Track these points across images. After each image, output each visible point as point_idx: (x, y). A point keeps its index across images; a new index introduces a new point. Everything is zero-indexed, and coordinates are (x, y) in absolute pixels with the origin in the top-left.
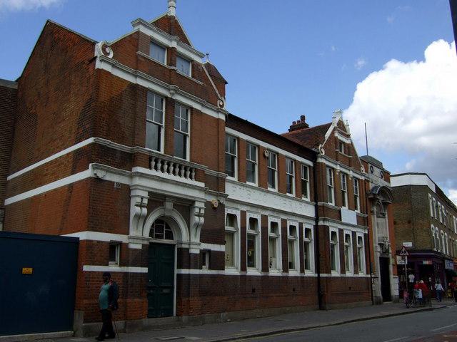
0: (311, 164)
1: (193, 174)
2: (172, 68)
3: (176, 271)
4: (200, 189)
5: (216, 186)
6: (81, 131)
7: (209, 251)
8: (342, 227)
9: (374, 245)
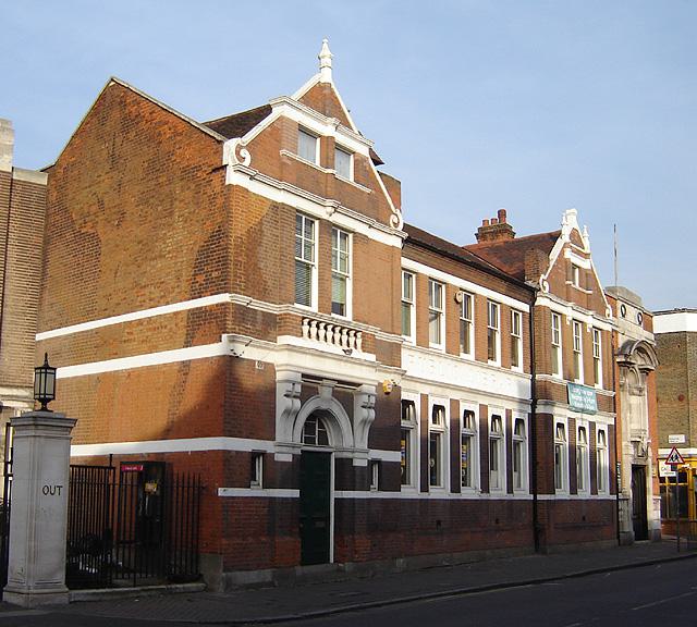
0: (526, 308)
1: (359, 342)
2: (330, 171)
3: (334, 494)
4: (371, 365)
5: (390, 356)
6: (201, 279)
7: (379, 462)
8: (573, 415)
9: (624, 443)
